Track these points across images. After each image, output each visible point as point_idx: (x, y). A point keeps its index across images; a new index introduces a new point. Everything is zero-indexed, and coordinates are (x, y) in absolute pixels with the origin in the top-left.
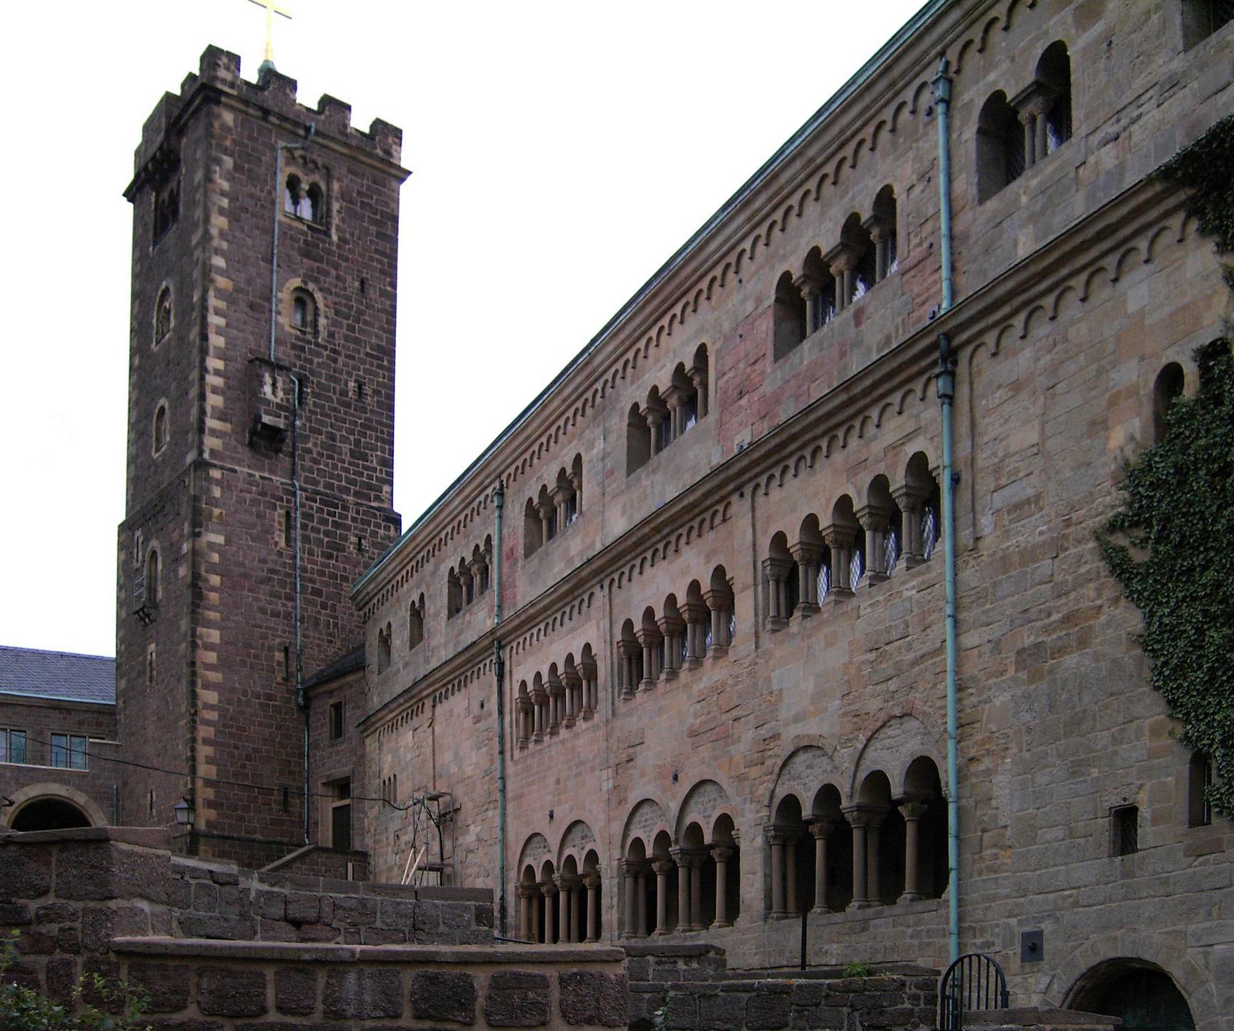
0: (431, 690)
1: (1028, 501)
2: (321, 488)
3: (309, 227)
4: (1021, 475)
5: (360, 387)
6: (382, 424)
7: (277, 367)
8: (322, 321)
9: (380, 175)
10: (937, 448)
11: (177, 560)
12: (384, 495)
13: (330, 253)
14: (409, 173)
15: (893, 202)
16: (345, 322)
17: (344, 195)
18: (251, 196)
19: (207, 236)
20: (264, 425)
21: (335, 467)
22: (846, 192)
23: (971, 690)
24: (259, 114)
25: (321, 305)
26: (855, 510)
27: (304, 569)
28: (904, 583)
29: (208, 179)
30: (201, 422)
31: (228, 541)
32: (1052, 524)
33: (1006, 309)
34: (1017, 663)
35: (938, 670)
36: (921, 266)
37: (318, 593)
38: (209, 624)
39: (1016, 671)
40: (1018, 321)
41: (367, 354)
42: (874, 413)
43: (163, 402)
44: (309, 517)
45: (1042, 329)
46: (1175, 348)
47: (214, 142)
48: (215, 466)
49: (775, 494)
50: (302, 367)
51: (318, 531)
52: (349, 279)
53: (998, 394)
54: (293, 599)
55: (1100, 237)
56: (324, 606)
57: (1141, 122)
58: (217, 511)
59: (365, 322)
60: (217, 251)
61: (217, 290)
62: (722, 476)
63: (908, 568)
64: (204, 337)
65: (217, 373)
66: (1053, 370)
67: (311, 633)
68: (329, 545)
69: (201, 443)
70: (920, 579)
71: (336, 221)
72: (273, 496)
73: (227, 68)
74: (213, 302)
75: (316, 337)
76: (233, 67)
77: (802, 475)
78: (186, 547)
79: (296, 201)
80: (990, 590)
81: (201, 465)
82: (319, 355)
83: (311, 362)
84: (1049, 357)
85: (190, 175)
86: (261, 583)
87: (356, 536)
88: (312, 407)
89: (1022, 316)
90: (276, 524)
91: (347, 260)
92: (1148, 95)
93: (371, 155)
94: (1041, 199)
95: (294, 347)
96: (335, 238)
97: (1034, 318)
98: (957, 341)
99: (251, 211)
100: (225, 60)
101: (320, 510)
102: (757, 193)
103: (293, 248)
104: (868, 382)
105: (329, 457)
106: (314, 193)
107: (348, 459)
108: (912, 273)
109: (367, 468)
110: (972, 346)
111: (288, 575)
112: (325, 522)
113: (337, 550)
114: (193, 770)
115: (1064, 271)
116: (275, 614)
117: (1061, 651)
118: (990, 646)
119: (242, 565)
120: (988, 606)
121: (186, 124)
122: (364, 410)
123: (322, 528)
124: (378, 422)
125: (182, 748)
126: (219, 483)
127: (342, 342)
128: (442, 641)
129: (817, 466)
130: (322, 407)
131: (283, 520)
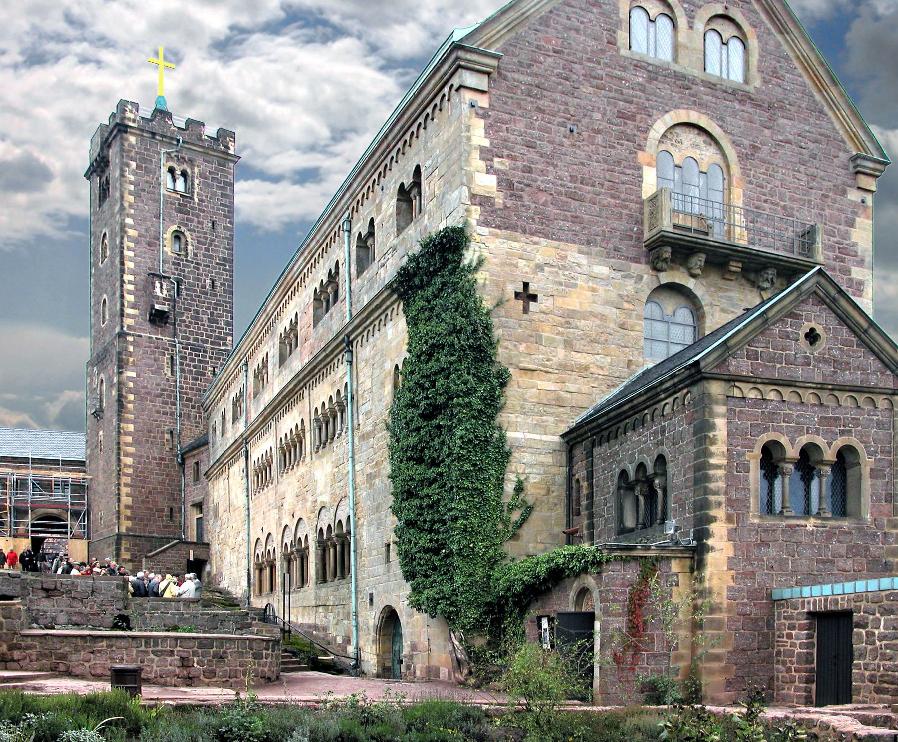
3: (181, 195)
5: (213, 283)
6: (226, 302)
7: (161, 278)
8: (190, 247)
9: (222, 161)
11: (112, 386)
12: (228, 342)
13: (193, 208)
17: (201, 175)
18: (147, 182)
19: (122, 208)
20: (156, 310)
21: (199, 329)
24: (150, 135)
25: (189, 239)
27: (181, 388)
29: (122, 175)
30: (122, 310)
31: (138, 375)
37: (190, 400)
38: (128, 421)
41: (217, 264)
43: (105, 296)
44: (184, 358)
48: (130, 335)
51: (190, 366)
52: (205, 222)
54: (175, 404)
56: (193, 407)
58: (131, 359)
59: (215, 246)
60: (128, 215)
61: (129, 236)
65: (130, 283)
67: (185, 422)
68: (196, 373)
69: (122, 322)
71: (196, 190)
73: (131, 112)
74: (127, 243)
75: (186, 257)
78: (115, 380)
79: (174, 180)
81: (122, 335)
82: (189, 267)
83: (184, 271)
85: (114, 172)
91: (203, 211)
95: (174, 264)
96: (196, 200)
99: (147, 190)
100: (130, 107)
101: (191, 354)
103: (172, 208)
105: (196, 324)
106: (184, 174)
107: (206, 324)
109: (218, 328)
111: (172, 391)
112: (194, 360)
114: (119, 501)
116: (165, 413)
119: (146, 387)
121: (110, 143)
122: (216, 296)
125: (114, 488)
126: (132, 343)
131: (169, 361)
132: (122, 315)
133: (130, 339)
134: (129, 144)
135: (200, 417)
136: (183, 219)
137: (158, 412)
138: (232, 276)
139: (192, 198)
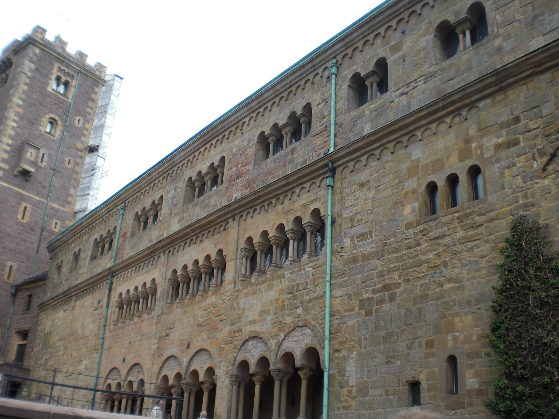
0: (75, 293)
1: (366, 234)
4: (363, 222)
10: (324, 208)
15: (311, 109)
22: (290, 104)
23: (337, 317)
26: (286, 230)
28: (307, 264)
32: (377, 245)
33: (359, 153)
34: (359, 306)
35: (321, 306)
36: (321, 134)
39: (359, 309)
40: (364, 159)
42: (297, 190)
45: (374, 164)
46: (433, 175)
49: (249, 221)
53: (354, 187)
55: (400, 129)
57: (418, 88)
62: (226, 210)
63: (309, 258)
66: (378, 179)
70: (314, 263)
77: (262, 213)
80: (347, 271)
84: (377, 174)
89: (365, 157)
92: (420, 79)
94: (374, 113)
97: (370, 158)
98: (336, 165)
102: (254, 100)
104: (295, 177)
108: (318, 136)
110: (343, 167)
115: (385, 141)
117: (380, 302)
118: (346, 297)
120: (346, 278)
128: (85, 271)
129: (270, 210)
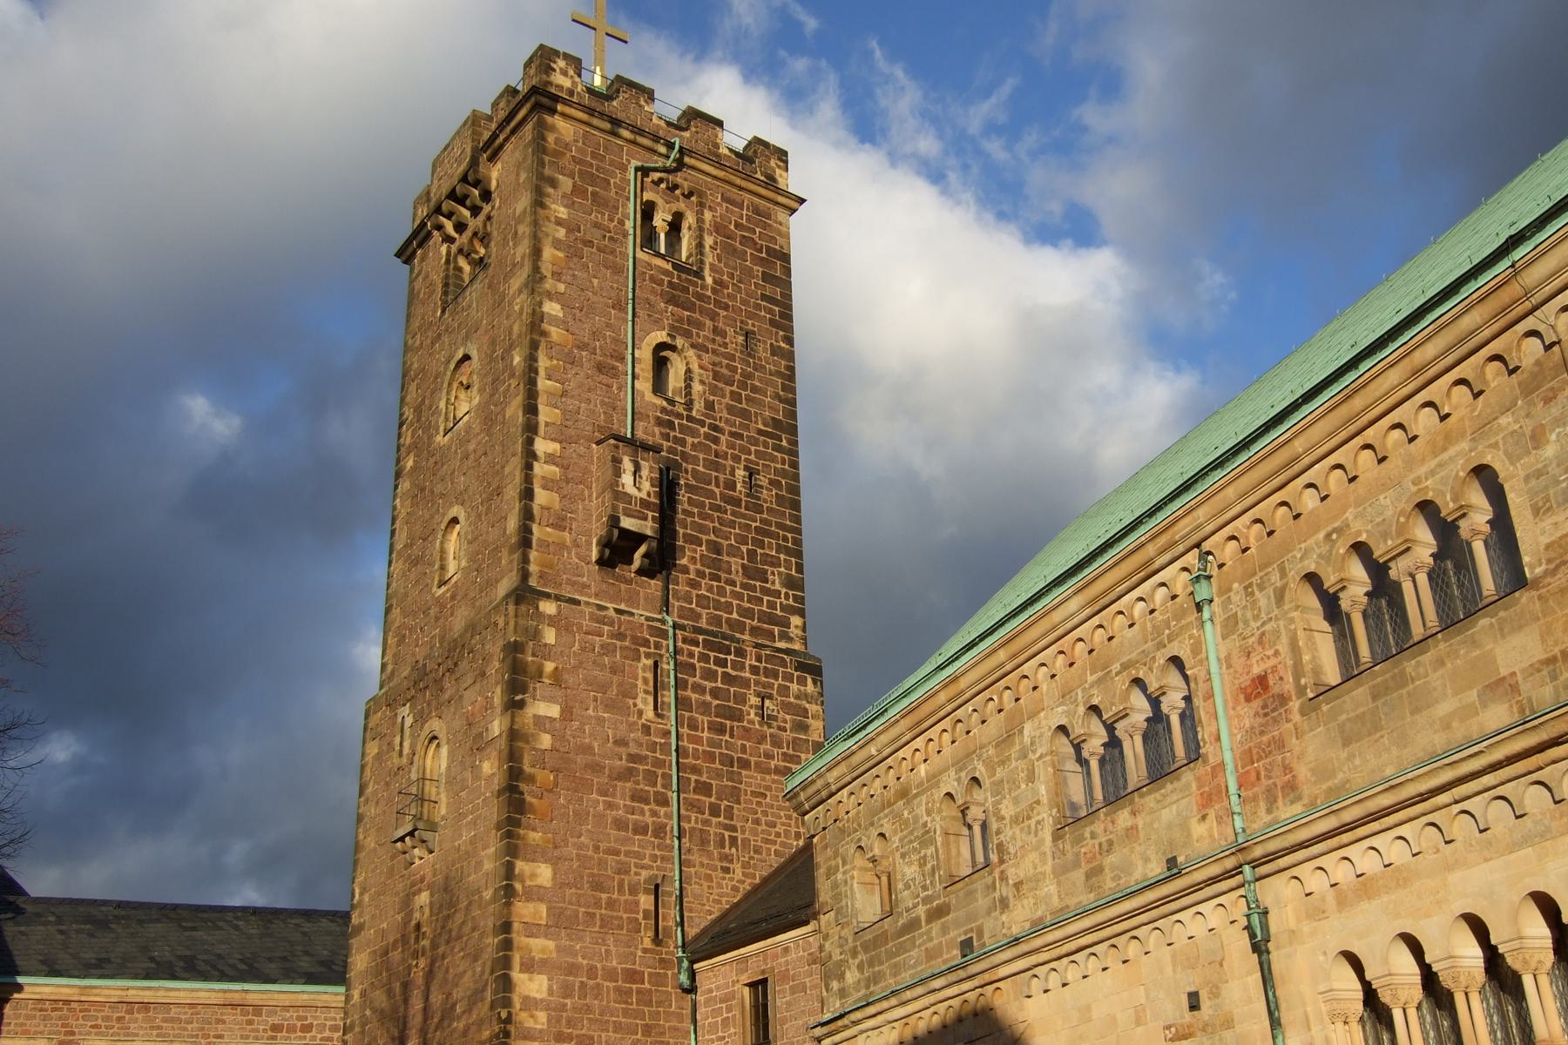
2: (703, 624)
12: (794, 632)
13: (701, 297)
14: (802, 201)
16: (728, 389)
18: (597, 225)
21: (721, 591)
24: (608, 126)
31: (567, 714)
37: (705, 789)
41: (760, 432)
47: (547, 159)
50: (671, 450)
51: (702, 690)
52: (730, 331)
56: (715, 811)
59: (755, 389)
60: (550, 296)
64: (531, 409)
65: (551, 459)
71: (709, 258)
72: (635, 640)
73: (565, 73)
75: (690, 410)
76: (571, 72)
82: (694, 434)
83: (683, 442)
86: (619, 778)
87: (758, 695)
88: (686, 506)
90: (640, 683)
93: (749, 177)
95: (659, 422)
96: (709, 280)
100: (561, 63)
101: (704, 658)
107: (739, 579)
113: (731, 718)
116: (641, 829)
119: (587, 749)
122: (758, 509)
123: (709, 685)
124: (779, 525)
126: (553, 621)
127: (725, 415)
130: (701, 505)
131: (650, 676)
132: (525, 542)
133: (548, 607)
134: (557, 141)
135: (733, 840)
136: (680, 320)
137: (620, 825)
138: (795, 465)
139: (699, 274)
